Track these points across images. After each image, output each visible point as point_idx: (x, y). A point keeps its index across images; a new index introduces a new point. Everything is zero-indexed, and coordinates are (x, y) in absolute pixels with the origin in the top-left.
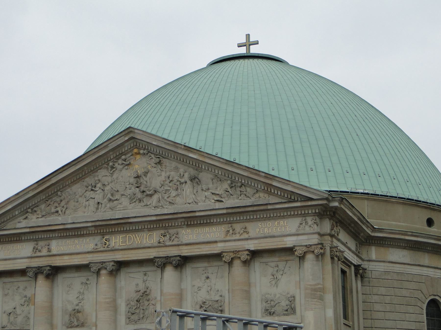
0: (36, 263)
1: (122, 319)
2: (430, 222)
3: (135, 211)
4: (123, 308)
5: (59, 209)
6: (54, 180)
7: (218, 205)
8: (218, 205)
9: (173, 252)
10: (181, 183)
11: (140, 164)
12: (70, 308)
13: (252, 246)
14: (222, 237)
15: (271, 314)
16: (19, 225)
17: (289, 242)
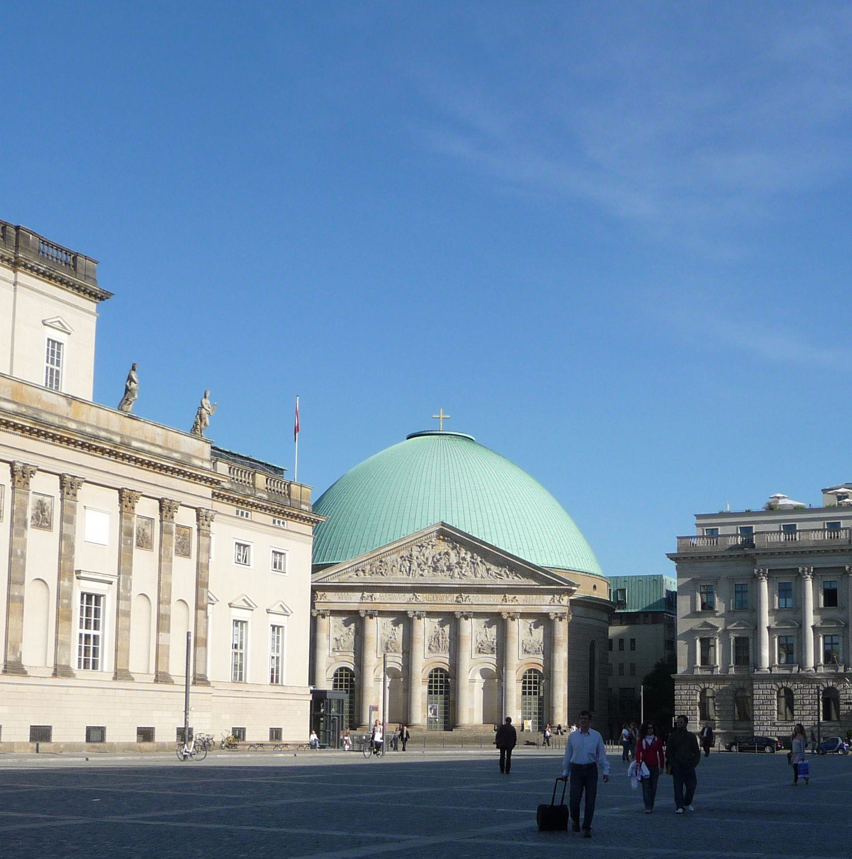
0: (363, 608)
1: (427, 648)
2: (595, 587)
3: (442, 579)
4: (427, 643)
5: (383, 571)
6: (382, 551)
7: (499, 581)
8: (499, 581)
9: (467, 609)
10: (473, 563)
11: (443, 547)
12: (386, 639)
13: (520, 609)
14: (500, 602)
15: (528, 652)
16: (351, 580)
17: (545, 609)
